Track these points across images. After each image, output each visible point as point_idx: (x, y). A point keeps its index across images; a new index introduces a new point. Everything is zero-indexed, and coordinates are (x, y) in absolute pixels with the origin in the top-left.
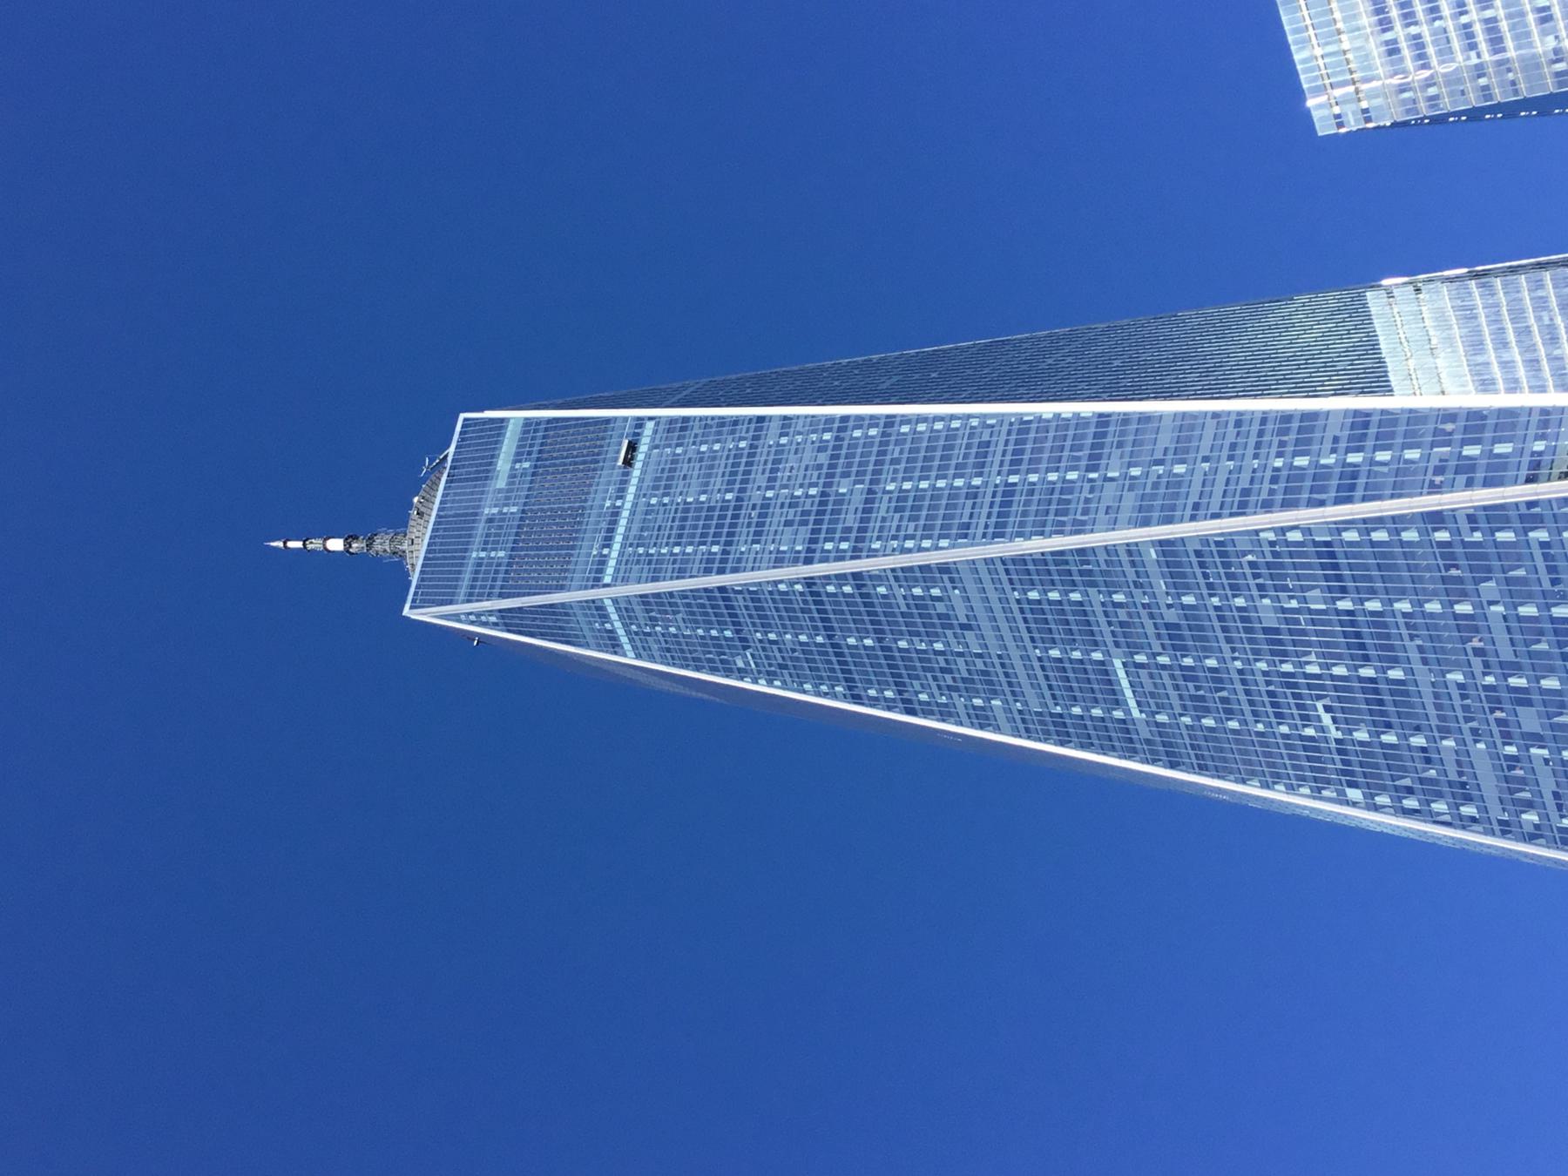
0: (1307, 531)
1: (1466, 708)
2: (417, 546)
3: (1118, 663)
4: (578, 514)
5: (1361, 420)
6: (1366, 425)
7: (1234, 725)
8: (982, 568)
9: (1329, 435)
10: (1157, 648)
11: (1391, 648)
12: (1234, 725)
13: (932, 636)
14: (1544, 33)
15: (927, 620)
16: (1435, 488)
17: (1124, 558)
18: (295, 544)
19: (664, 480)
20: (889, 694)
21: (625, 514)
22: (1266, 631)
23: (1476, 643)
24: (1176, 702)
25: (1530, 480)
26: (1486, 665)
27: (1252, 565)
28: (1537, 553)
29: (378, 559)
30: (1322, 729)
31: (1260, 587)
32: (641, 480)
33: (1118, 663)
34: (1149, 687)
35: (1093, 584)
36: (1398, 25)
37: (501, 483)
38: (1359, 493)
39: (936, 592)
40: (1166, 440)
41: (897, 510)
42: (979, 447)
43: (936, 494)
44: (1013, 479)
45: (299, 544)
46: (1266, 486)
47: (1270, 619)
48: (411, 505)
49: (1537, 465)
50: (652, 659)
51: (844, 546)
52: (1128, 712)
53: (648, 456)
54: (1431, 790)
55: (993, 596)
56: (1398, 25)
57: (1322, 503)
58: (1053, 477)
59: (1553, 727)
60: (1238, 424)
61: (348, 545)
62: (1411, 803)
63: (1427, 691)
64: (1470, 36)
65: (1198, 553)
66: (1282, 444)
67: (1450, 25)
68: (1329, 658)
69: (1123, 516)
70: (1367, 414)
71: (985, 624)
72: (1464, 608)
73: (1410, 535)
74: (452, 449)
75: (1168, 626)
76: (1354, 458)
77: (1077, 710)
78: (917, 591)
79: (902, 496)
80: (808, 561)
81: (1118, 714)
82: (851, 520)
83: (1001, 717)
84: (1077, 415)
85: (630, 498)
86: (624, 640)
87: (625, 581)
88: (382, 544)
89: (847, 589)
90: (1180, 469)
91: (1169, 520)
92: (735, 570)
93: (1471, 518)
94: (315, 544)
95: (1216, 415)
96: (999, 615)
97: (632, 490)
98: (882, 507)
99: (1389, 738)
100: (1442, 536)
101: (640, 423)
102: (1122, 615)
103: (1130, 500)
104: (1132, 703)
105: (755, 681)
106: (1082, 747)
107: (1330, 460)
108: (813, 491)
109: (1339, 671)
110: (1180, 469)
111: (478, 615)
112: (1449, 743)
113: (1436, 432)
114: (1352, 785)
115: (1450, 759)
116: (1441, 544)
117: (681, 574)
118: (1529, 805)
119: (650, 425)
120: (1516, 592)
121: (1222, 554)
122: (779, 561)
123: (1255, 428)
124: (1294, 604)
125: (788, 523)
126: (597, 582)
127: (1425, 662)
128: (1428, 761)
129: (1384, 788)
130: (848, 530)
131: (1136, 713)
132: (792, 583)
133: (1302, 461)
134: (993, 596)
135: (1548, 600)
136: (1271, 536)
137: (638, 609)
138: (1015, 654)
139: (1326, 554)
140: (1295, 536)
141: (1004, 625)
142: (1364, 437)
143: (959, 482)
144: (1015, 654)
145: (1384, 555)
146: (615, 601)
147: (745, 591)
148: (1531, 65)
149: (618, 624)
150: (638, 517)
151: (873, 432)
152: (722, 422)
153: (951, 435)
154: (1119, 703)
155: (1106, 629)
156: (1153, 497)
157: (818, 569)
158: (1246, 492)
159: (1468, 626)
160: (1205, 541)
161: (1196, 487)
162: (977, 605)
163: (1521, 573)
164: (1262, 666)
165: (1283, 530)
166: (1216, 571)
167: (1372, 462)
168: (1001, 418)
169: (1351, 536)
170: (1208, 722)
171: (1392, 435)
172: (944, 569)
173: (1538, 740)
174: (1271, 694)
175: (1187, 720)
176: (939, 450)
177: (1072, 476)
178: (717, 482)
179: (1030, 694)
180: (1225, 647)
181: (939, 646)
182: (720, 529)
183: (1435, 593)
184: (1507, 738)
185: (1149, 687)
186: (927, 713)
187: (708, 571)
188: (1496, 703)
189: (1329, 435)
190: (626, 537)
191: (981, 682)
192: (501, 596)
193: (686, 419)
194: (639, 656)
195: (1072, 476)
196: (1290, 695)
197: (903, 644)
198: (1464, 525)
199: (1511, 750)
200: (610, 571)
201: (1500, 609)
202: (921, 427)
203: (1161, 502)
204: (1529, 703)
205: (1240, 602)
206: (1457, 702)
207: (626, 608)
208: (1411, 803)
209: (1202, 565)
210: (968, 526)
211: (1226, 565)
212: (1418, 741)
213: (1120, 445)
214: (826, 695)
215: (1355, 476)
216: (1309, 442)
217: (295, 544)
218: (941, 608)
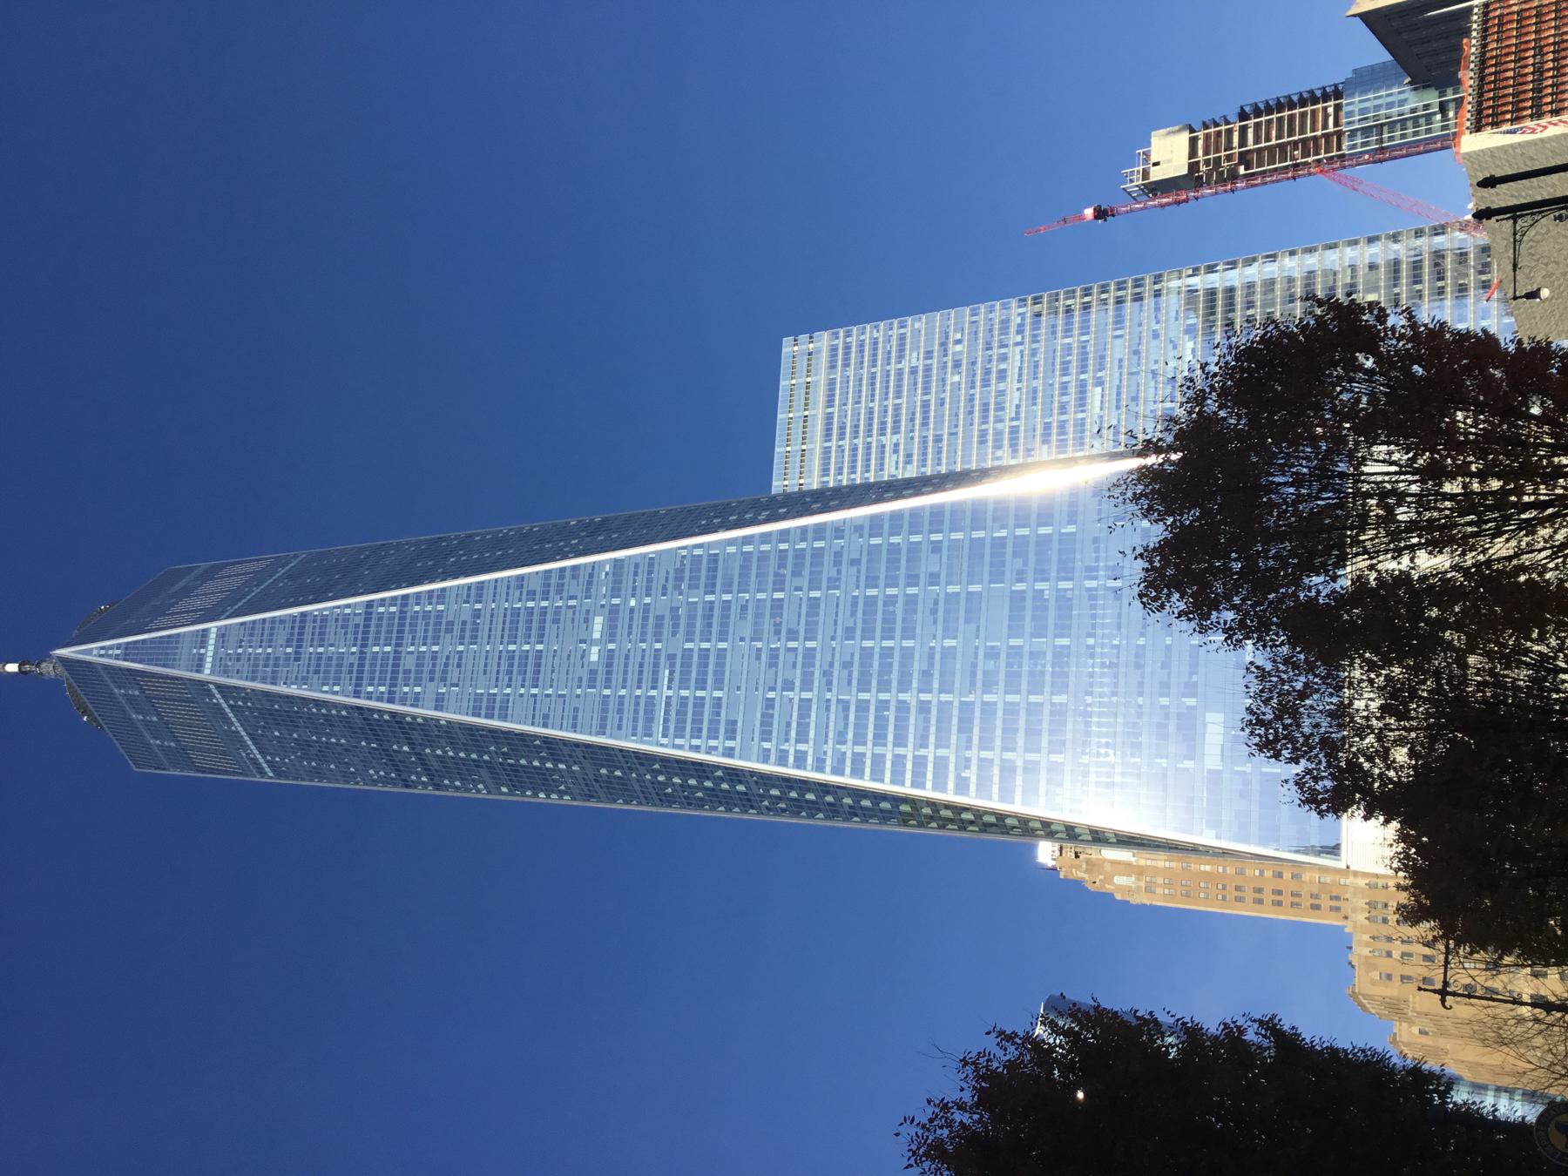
89: (393, 609)
136: (684, 553)
149: (211, 648)
159: (777, 605)
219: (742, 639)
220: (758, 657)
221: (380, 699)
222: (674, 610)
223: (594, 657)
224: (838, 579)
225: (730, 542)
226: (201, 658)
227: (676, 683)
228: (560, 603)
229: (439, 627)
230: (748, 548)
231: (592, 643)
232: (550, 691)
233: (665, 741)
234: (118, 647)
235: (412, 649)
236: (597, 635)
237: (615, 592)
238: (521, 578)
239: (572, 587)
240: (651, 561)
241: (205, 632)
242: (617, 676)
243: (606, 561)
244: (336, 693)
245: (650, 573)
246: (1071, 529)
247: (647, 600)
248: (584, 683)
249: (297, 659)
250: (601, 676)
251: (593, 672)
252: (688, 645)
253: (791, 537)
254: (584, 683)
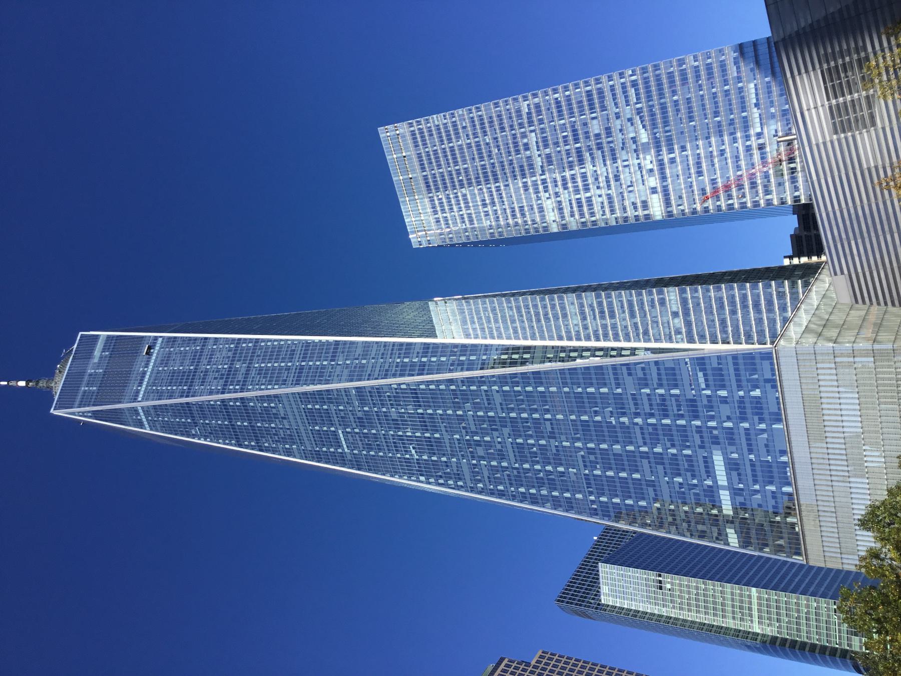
0: (408, 385)
1: (460, 447)
2: (58, 385)
3: (340, 432)
4: (129, 373)
5: (426, 346)
6: (428, 348)
7: (381, 454)
8: (291, 396)
9: (416, 351)
10: (354, 426)
11: (435, 426)
12: (381, 454)
13: (271, 422)
14: (486, 220)
15: (268, 415)
16: (451, 371)
17: (343, 393)
19: (165, 360)
20: (253, 443)
21: (148, 373)
22: (393, 420)
23: (463, 425)
24: (361, 446)
25: (482, 369)
26: (467, 432)
27: (389, 396)
28: (483, 393)
29: (40, 390)
30: (412, 455)
31: (391, 404)
32: (156, 360)
33: (340, 432)
34: (351, 441)
35: (332, 403)
36: (440, 213)
37: (96, 360)
38: (425, 372)
39: (272, 405)
40: (359, 351)
41: (259, 374)
42: (291, 351)
43: (274, 368)
44: (303, 364)
45: (6, 383)
46: (394, 369)
47: (394, 416)
48: (56, 368)
49: (483, 364)
50: (157, 430)
51: (237, 387)
52: (343, 450)
53: (159, 351)
54: (448, 476)
55: (294, 406)
56: (440, 213)
57: (413, 375)
58: (318, 363)
59: (488, 454)
60: (385, 346)
61: (27, 384)
62: (441, 481)
63: (447, 441)
64: (463, 218)
65: (370, 392)
66: (400, 354)
67: (456, 214)
68: (414, 430)
69: (343, 378)
70: (429, 344)
71: (291, 417)
72: (460, 413)
73: (442, 387)
74: (75, 346)
75: (358, 418)
76: (424, 359)
77: (324, 449)
78: (265, 405)
79: (261, 369)
80: (223, 393)
81: (340, 450)
82: (240, 377)
83: (296, 453)
84: (327, 341)
85: (150, 367)
86: (146, 423)
87: (147, 400)
88: (42, 384)
89: (238, 404)
90: (364, 362)
91: (360, 380)
92: (193, 396)
93: (462, 382)
94: (13, 383)
95: (377, 343)
96: (297, 414)
97: (152, 364)
98: (253, 373)
99: (434, 458)
100: (453, 387)
101: (156, 338)
102: (342, 414)
103: (346, 372)
104: (345, 446)
105: (199, 439)
106: (326, 463)
107: (416, 360)
108: (226, 366)
109: (418, 434)
110: (364, 362)
111: (83, 413)
112: (454, 460)
113: (451, 351)
114: (422, 475)
115: (454, 465)
116: (453, 390)
117: (170, 397)
118: (480, 481)
119: (160, 339)
120: (477, 407)
121: (378, 392)
122: (211, 393)
123: (391, 348)
124: (403, 410)
125: (215, 378)
126: (135, 400)
127: (447, 431)
128: (447, 466)
129: (432, 476)
130: (239, 381)
131: (346, 450)
132: (216, 401)
133: (406, 360)
134: (294, 406)
135: (487, 410)
136: (395, 386)
137: (152, 411)
138: (302, 428)
139: (414, 393)
140: (403, 386)
141: (298, 417)
142: (427, 352)
143: (283, 364)
144: (302, 428)
145: (433, 394)
146: (142, 408)
147: (197, 404)
148: (482, 230)
149: (143, 417)
150: (154, 375)
151: (250, 345)
152: (190, 339)
153: (280, 347)
154: (340, 446)
155: (336, 419)
156: (354, 371)
157: (227, 396)
158: (387, 371)
159: (461, 419)
160: (372, 387)
161: (370, 369)
162: (288, 410)
163: (478, 400)
164: (392, 433)
165: (400, 384)
166: (376, 399)
167: (430, 361)
168: (299, 341)
169: (422, 387)
170: (372, 453)
171: (437, 352)
172: (276, 396)
173: (483, 458)
174: (394, 443)
175: (364, 452)
176: (276, 352)
177: (325, 363)
178: (187, 362)
179: (307, 443)
180: (379, 426)
181: (273, 425)
182: (187, 380)
183: (450, 407)
184: (473, 458)
185: (351, 441)
186: (267, 451)
187: (182, 396)
188: (470, 446)
189: (416, 351)
190: (148, 383)
191: (289, 439)
192: (94, 405)
193: (175, 338)
194: (151, 430)
195: (325, 363)
196: (401, 443)
197: (259, 425)
198: (460, 384)
199: (474, 462)
200: (141, 396)
201: (471, 413)
202: (269, 344)
203: (357, 373)
204: (480, 445)
205: (384, 410)
206: (457, 445)
207: (146, 411)
208: (441, 481)
209: (371, 396)
210: (286, 380)
211: (380, 396)
212: (444, 459)
213: (343, 352)
214: (227, 444)
215: (424, 366)
216: (409, 353)
218: (274, 411)
234: (89, 412)
246: (619, 391)
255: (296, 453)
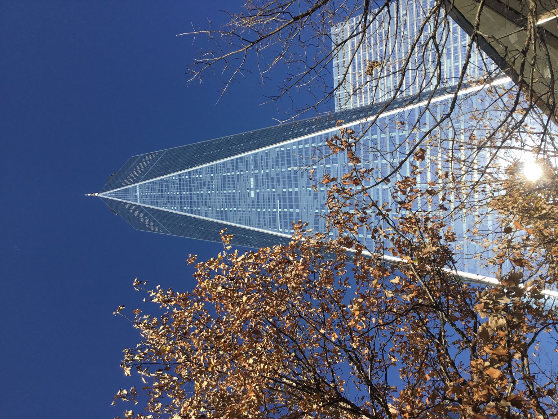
18: (89, 195)
94: (93, 195)
136: (278, 149)
146: (139, 186)
169: (295, 147)
186: (195, 213)
217: (89, 195)
219: (303, 187)
220: (310, 195)
221: (188, 212)
222: (277, 175)
223: (253, 196)
224: (336, 159)
225: (294, 144)
226: (136, 196)
227: (282, 207)
228: (238, 173)
229: (202, 184)
230: (301, 147)
231: (251, 189)
232: (240, 210)
233: (281, 230)
234: (113, 193)
235: (195, 193)
236: (252, 186)
237: (256, 168)
238: (224, 163)
239: (242, 166)
240: (267, 154)
241: (136, 186)
242: (261, 203)
243: (251, 154)
244: (175, 210)
245: (267, 159)
247: (267, 171)
248: (250, 206)
249: (162, 197)
250: (256, 203)
251: (253, 202)
252: (285, 190)
253: (316, 141)
254: (250, 206)
255: (210, 215)
